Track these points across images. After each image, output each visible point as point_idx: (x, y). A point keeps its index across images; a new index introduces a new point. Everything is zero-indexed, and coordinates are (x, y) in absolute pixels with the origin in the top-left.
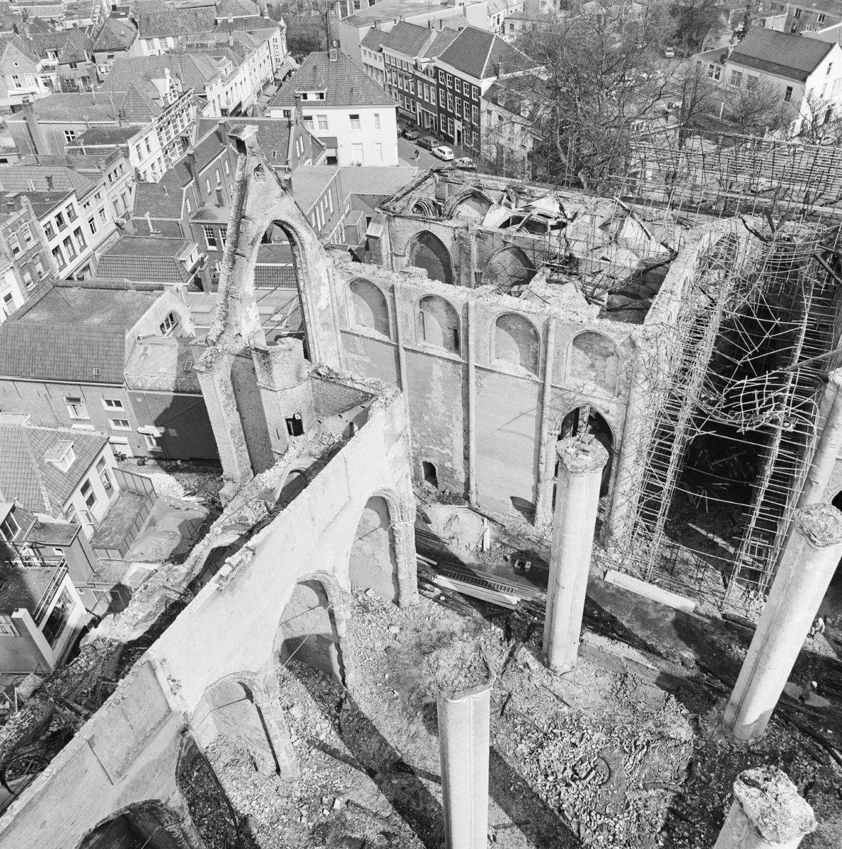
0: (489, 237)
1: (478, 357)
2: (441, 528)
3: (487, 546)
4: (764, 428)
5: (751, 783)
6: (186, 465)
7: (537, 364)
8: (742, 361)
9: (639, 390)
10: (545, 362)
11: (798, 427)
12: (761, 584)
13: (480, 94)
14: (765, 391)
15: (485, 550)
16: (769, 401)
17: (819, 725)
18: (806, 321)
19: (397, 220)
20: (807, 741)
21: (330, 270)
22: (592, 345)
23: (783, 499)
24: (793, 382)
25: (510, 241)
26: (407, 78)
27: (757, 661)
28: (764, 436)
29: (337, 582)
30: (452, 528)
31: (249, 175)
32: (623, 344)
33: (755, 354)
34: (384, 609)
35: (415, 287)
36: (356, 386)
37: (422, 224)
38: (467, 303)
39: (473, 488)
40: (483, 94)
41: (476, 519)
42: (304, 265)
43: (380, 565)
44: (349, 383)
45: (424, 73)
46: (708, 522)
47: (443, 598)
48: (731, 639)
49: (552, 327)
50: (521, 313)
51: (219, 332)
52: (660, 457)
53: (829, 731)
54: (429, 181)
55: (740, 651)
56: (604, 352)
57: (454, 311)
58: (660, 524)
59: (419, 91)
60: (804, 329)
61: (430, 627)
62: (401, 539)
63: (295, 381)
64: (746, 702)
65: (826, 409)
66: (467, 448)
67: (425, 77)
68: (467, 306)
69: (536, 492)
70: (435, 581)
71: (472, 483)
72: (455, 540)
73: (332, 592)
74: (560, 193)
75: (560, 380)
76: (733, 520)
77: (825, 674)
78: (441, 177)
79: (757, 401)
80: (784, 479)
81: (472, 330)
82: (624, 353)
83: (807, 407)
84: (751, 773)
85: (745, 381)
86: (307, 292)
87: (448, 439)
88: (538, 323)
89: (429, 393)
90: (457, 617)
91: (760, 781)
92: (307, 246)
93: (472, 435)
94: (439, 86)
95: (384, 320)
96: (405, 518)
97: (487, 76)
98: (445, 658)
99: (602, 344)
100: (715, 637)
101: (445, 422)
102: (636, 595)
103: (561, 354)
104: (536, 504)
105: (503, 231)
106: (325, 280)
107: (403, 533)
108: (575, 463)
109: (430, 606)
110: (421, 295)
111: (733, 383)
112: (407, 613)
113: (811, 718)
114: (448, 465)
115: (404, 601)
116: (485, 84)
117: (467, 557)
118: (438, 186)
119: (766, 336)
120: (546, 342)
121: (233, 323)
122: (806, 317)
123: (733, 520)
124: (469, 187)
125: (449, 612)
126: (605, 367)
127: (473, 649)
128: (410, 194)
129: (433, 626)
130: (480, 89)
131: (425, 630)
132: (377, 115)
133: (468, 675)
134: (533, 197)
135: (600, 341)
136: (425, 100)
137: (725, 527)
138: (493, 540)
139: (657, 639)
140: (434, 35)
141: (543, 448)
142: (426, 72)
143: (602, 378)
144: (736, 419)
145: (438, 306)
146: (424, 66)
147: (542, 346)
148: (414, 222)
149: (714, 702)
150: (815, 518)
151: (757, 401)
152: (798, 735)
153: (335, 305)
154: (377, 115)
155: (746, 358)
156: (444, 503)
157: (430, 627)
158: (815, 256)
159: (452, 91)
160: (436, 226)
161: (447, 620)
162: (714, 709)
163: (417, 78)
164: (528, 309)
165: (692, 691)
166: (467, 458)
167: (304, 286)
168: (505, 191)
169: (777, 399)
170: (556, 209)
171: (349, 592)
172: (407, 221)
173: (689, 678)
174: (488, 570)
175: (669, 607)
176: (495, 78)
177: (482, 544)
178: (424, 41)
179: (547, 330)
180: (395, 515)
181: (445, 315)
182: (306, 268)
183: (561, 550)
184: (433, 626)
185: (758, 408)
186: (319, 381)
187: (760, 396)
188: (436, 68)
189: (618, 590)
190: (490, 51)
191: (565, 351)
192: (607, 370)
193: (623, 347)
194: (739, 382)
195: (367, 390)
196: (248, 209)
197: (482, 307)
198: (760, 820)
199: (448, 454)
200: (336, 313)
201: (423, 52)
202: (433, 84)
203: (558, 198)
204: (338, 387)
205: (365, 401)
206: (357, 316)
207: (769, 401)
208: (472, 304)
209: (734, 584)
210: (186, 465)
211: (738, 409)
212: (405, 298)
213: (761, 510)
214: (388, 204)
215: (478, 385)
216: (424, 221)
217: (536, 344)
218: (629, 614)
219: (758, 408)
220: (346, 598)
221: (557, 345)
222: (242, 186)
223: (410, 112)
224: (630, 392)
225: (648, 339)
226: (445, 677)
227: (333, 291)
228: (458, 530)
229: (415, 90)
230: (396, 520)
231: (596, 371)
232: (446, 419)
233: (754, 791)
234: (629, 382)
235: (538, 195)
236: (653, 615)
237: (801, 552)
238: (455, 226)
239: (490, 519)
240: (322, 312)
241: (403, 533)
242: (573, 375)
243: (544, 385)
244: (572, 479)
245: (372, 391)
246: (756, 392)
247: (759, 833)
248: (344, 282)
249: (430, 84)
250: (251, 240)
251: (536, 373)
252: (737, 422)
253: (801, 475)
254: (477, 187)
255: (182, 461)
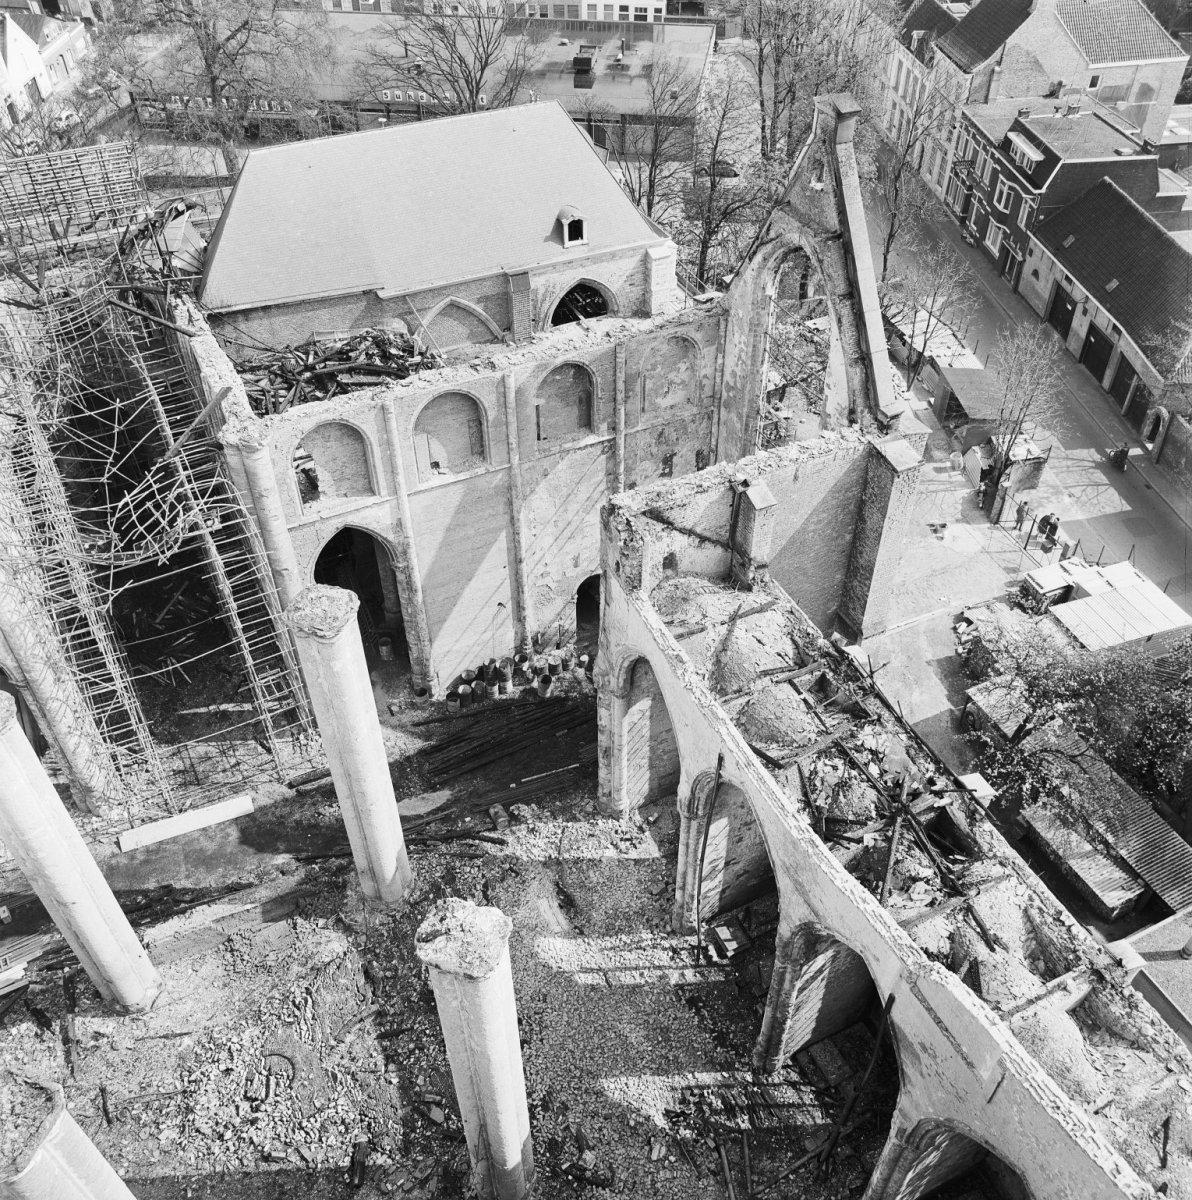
4: (187, 542)
5: (429, 938)
8: (106, 475)
11: (224, 518)
12: (304, 721)
14: (158, 497)
16: (172, 507)
17: (455, 821)
18: (152, 387)
20: (455, 847)
23: (262, 610)
24: (185, 469)
27: (355, 807)
28: (192, 552)
33: (117, 459)
46: (199, 693)
48: (314, 804)
52: (85, 653)
53: (468, 819)
55: (332, 810)
58: (143, 735)
60: (157, 398)
64: (374, 858)
65: (241, 480)
76: (225, 671)
77: (427, 767)
79: (157, 515)
80: (249, 588)
83: (219, 489)
84: (425, 928)
85: (127, 499)
91: (438, 927)
100: (297, 816)
102: (174, 840)
111: (114, 509)
113: (444, 820)
119: (116, 431)
122: (150, 382)
123: (225, 671)
137: (222, 685)
139: (235, 869)
144: (147, 549)
149: (344, 886)
150: (308, 611)
151: (157, 515)
152: (443, 848)
155: (110, 470)
158: (110, 303)
162: (349, 892)
165: (313, 894)
169: (180, 498)
173: (300, 884)
175: (223, 823)
185: (164, 523)
187: (157, 506)
189: (148, 851)
194: (120, 504)
198: (464, 965)
207: (172, 507)
209: (276, 743)
211: (142, 537)
213: (248, 639)
218: (183, 868)
219: (164, 523)
233: (440, 941)
236: (210, 847)
237: (318, 657)
246: (149, 504)
247: (471, 977)
252: (150, 553)
253: (263, 571)
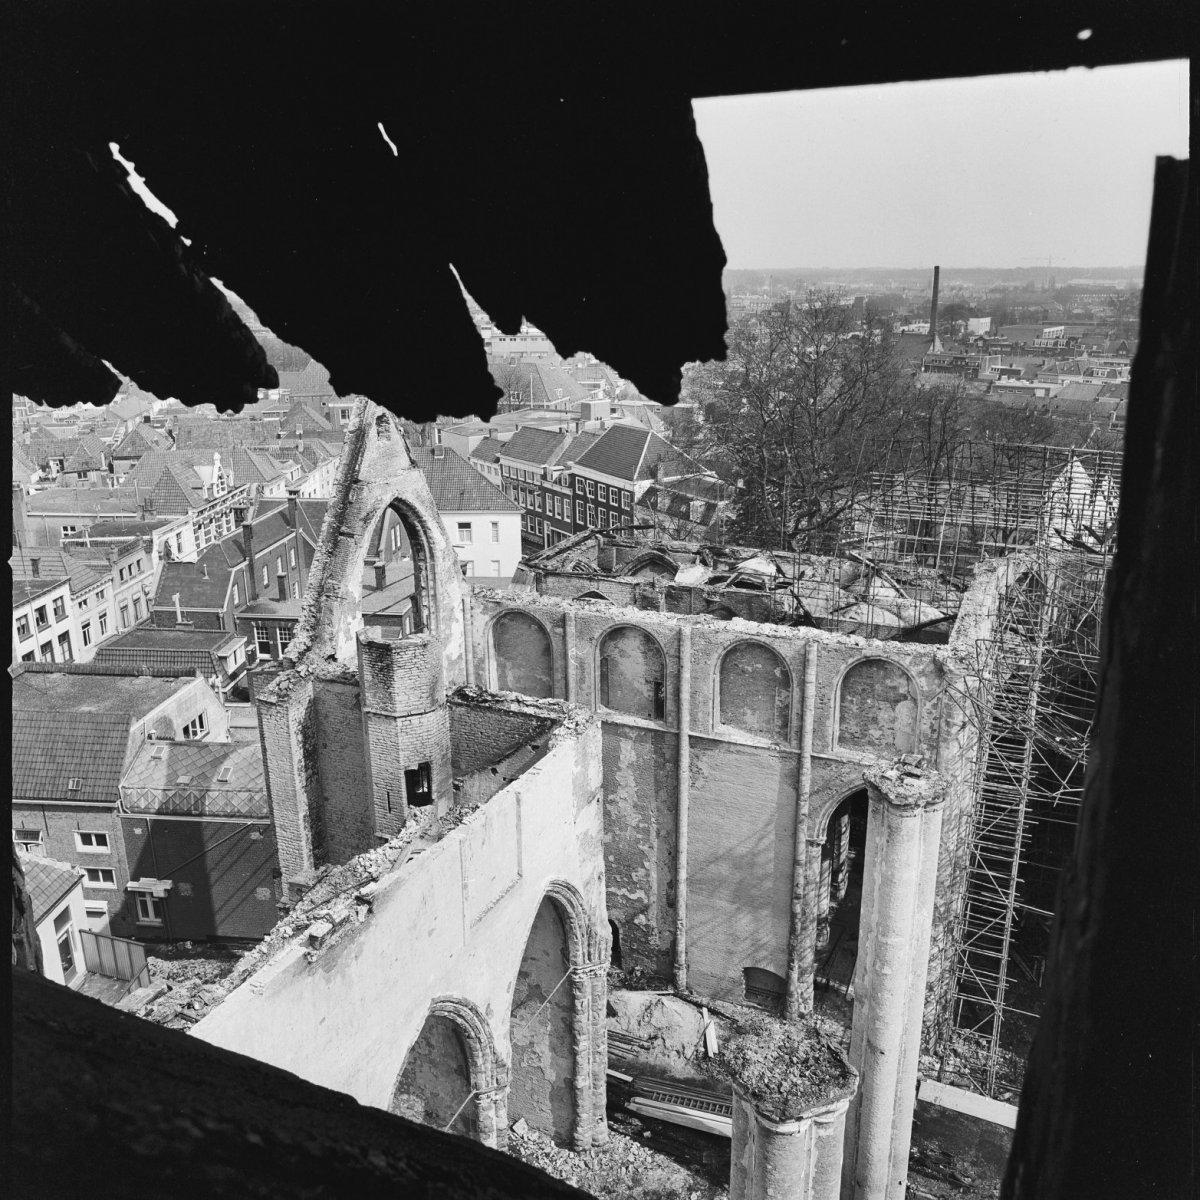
0: (685, 595)
1: (694, 721)
2: (634, 1022)
3: (713, 1047)
6: (199, 949)
7: (787, 726)
9: (954, 749)
10: (801, 717)
13: (632, 500)
15: (711, 1054)
19: (550, 580)
21: (467, 600)
22: (872, 686)
25: (717, 599)
26: (531, 492)
29: (490, 1037)
30: (653, 1021)
31: (370, 425)
32: (922, 673)
34: (547, 1155)
35: (598, 614)
36: (526, 710)
37: (586, 583)
38: (680, 633)
39: (682, 958)
40: (636, 500)
41: (689, 1011)
42: (431, 583)
43: (542, 1065)
44: (514, 707)
45: (555, 482)
47: (647, 1134)
49: (813, 656)
50: (763, 639)
51: (303, 647)
54: (590, 542)
56: (892, 694)
57: (659, 652)
59: (548, 507)
61: (630, 1184)
62: (585, 1003)
63: (426, 703)
66: (673, 884)
67: (557, 488)
68: (679, 636)
69: (791, 951)
70: (632, 1107)
71: (681, 947)
72: (659, 1042)
73: (480, 1061)
74: (775, 553)
75: (825, 746)
78: (606, 539)
81: (686, 675)
82: (926, 688)
86: (433, 627)
87: (642, 872)
88: (786, 651)
89: (613, 792)
90: (676, 1166)
92: (438, 554)
93: (683, 859)
94: (576, 496)
95: (545, 678)
96: (595, 959)
97: (642, 477)
98: (755, 1047)
99: (888, 682)
101: (637, 841)
102: (976, 1120)
103: (826, 701)
104: (788, 976)
105: (707, 588)
106: (459, 615)
107: (588, 990)
108: (901, 790)
109: (627, 1149)
110: (606, 627)
112: (588, 1159)
114: (641, 919)
115: (584, 1135)
116: (641, 487)
117: (680, 1068)
118: (601, 550)
120: (803, 683)
121: (327, 637)
124: (646, 551)
125: (659, 1158)
126: (893, 721)
127: (802, 1035)
128: (565, 555)
129: (636, 1181)
130: (632, 494)
131: (621, 1189)
132: (495, 524)
133: (807, 1073)
134: (738, 559)
135: (885, 677)
136: (557, 517)
138: (721, 1042)
140: (568, 440)
141: (800, 871)
142: (558, 482)
143: (890, 740)
145: (632, 645)
146: (556, 475)
147: (796, 691)
148: (575, 582)
153: (470, 656)
154: (495, 524)
156: (631, 988)
157: (630, 1184)
159: (595, 502)
160: (607, 585)
161: (659, 1171)
163: (545, 490)
164: (774, 633)
166: (672, 903)
167: (428, 617)
168: (698, 553)
170: (771, 569)
171: (509, 1065)
172: (564, 580)
174: (720, 1086)
176: (652, 481)
177: (705, 1046)
178: (555, 446)
179: (804, 662)
180: (579, 951)
181: (641, 660)
182: (434, 588)
183: (879, 975)
184: (636, 1181)
186: (463, 710)
188: (573, 476)
189: (943, 1111)
190: (645, 450)
191: (833, 697)
192: (897, 725)
193: (923, 679)
195: (544, 714)
196: (364, 471)
197: (703, 635)
199: (639, 900)
200: (471, 670)
201: (554, 459)
202: (568, 496)
203: (773, 559)
204: (495, 716)
205: (540, 734)
206: (502, 677)
208: (687, 630)
210: (199, 949)
212: (580, 634)
214: (537, 561)
215: (696, 772)
216: (590, 579)
217: (784, 693)
220: (503, 1078)
221: (820, 687)
222: (357, 437)
223: (535, 535)
224: (938, 754)
225: (962, 660)
226: (762, 1077)
227: (469, 634)
228: (663, 1023)
229: (543, 506)
230: (580, 960)
231: (880, 729)
232: (640, 836)
234: (935, 736)
235: (744, 555)
238: (635, 582)
239: (713, 1012)
240: (452, 663)
241: (588, 990)
242: (842, 740)
243: (800, 757)
244: (895, 821)
245: (553, 716)
248: (487, 618)
249: (564, 496)
250: (363, 514)
251: (786, 738)
254: (658, 550)
255: (195, 943)
